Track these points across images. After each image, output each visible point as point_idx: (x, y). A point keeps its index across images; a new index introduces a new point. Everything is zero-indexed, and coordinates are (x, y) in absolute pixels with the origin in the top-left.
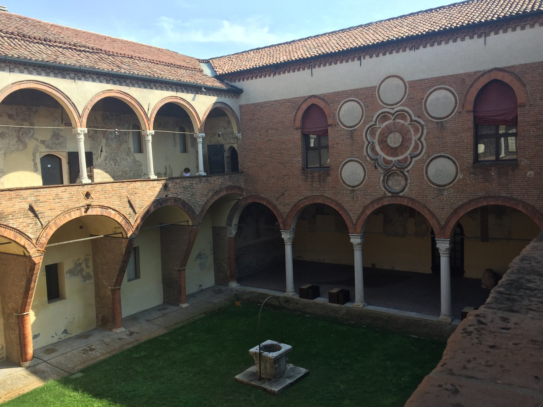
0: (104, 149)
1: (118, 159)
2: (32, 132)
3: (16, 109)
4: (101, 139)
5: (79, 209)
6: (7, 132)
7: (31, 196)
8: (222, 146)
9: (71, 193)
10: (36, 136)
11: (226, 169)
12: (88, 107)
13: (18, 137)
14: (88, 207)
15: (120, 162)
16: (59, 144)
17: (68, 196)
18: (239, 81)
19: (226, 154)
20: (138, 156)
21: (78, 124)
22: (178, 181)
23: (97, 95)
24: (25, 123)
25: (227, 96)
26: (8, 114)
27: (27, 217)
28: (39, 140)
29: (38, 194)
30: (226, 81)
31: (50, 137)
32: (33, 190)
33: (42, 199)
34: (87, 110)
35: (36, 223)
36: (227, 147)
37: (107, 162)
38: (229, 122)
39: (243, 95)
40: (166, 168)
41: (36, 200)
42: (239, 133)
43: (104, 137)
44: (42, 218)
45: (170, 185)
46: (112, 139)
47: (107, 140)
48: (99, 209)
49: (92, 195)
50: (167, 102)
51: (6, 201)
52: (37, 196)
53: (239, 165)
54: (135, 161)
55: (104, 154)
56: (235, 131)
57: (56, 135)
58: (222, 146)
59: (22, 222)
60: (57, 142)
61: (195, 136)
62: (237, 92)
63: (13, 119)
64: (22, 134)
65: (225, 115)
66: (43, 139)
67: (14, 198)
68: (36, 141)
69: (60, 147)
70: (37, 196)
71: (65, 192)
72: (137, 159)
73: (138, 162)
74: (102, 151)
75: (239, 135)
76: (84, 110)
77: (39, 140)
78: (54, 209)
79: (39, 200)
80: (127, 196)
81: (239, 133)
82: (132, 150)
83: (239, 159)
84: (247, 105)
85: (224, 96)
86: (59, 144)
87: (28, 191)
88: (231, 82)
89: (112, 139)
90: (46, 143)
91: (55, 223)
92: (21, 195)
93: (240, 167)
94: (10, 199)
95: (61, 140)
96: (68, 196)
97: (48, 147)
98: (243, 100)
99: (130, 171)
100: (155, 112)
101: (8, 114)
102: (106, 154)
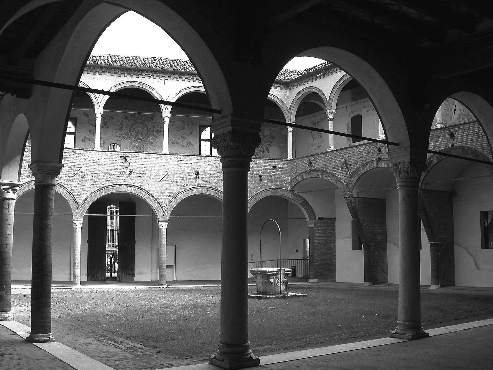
5: (372, 162)
14: (379, 160)
22: (468, 127)
27: (343, 169)
33: (351, 155)
35: (347, 173)
44: (350, 169)
48: (386, 162)
49: (382, 151)
59: (340, 172)
71: (365, 149)
74: (455, 110)
78: (358, 163)
79: (350, 156)
87: (345, 151)
91: (357, 173)
102: (460, 112)
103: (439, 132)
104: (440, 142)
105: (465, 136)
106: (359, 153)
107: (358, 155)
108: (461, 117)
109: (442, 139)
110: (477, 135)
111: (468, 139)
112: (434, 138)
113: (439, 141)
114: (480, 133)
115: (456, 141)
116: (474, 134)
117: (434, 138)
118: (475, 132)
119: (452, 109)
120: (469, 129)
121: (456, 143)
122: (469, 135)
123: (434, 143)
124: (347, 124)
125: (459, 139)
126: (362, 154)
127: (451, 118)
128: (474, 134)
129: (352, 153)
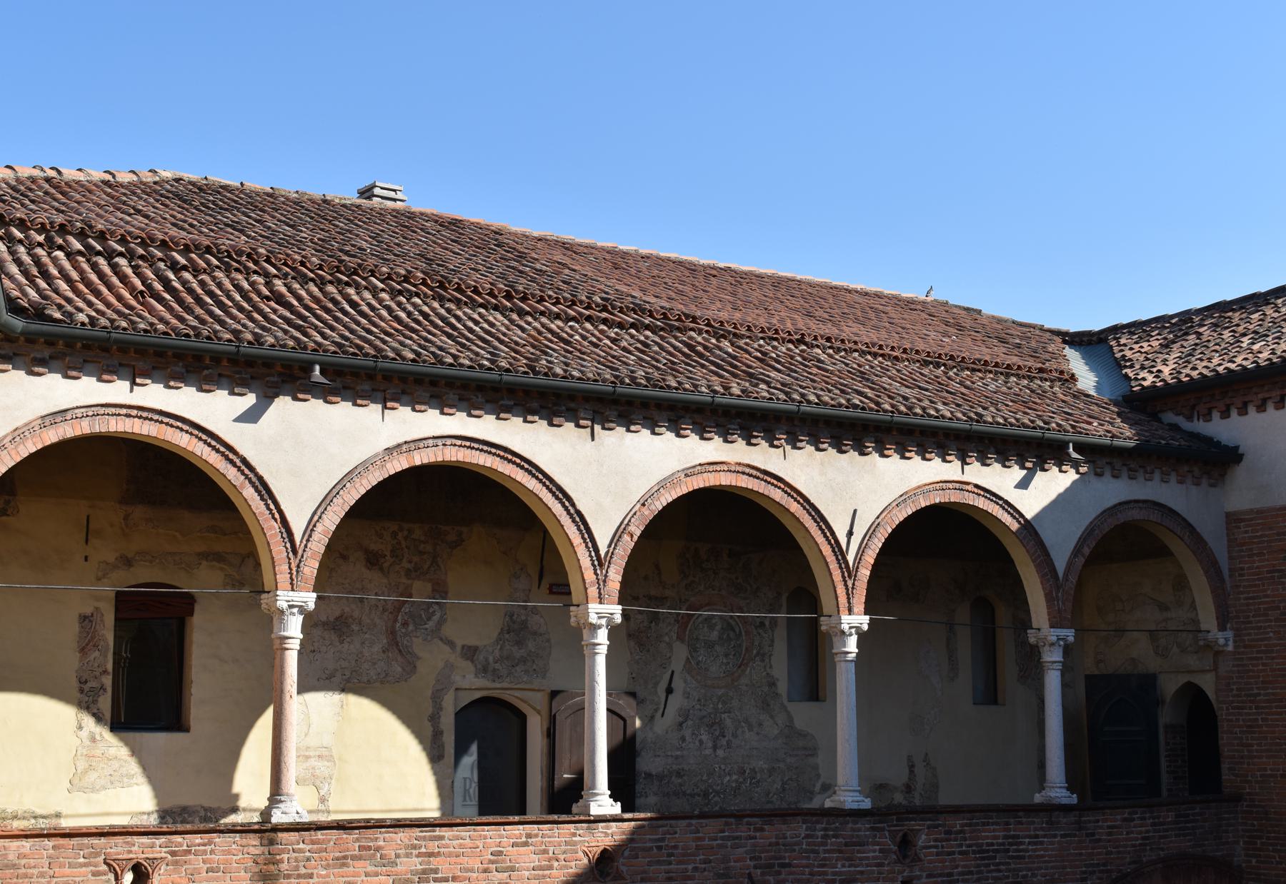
0: (678, 684)
1: (728, 722)
2: (436, 618)
3: (394, 535)
4: (670, 645)
6: (356, 614)
7: (407, 855)
8: (1149, 681)
9: (545, 852)
10: (448, 630)
11: (1165, 778)
12: (632, 528)
13: (392, 633)
15: (735, 736)
16: (523, 660)
17: (535, 860)
18: (1225, 414)
19: (1166, 717)
20: (803, 714)
21: (593, 591)
22: (957, 823)
23: (662, 485)
24: (417, 585)
25: (1173, 478)
26: (367, 552)
28: (459, 643)
29: (433, 846)
30: (1169, 417)
31: (495, 635)
32: (416, 832)
34: (626, 537)
36: (1170, 686)
37: (687, 733)
38: (1181, 583)
39: (1240, 473)
40: (911, 767)
41: (424, 872)
42: (1222, 628)
43: (680, 638)
45: (922, 840)
46: (710, 645)
47: (693, 649)
50: (923, 503)
51: (327, 867)
52: (431, 855)
53: (1225, 767)
54: (791, 732)
55: (676, 702)
56: (1208, 620)
57: (516, 629)
58: (1149, 681)
60: (518, 653)
61: (1032, 640)
62: (1219, 460)
63: (381, 569)
64: (405, 624)
65: (1163, 552)
66: (472, 641)
67: (354, 858)
68: (447, 648)
69: (526, 672)
70: (431, 855)
71: (526, 844)
72: (799, 724)
73: (802, 735)
74: (669, 691)
75: (1224, 639)
76: (615, 539)
77: (459, 643)
79: (436, 871)
80: (750, 875)
81: (1222, 628)
82: (782, 687)
83: (1224, 739)
84: (1260, 512)
85: (1157, 475)
86: (523, 660)
87: (403, 836)
88: (1190, 418)
89: (710, 645)
90: (481, 657)
92: (378, 849)
93: (1226, 776)
94: (342, 861)
95: (531, 645)
96: (535, 860)
97: (484, 670)
98: (1241, 494)
99: (772, 771)
100: (877, 543)
101: (367, 552)
103: (863, 826)
104: (867, 865)
105: (949, 854)
106: (492, 862)
107: (485, 871)
108: (690, 723)
109: (872, 852)
110: (983, 859)
111: (957, 867)
112: (846, 845)
113: (861, 859)
114: (993, 851)
115: (921, 870)
116: (974, 852)
117: (846, 845)
118: (977, 845)
119: (656, 684)
120: (961, 832)
121: (919, 878)
122: (961, 853)
123: (843, 866)
124: (84, 618)
125: (930, 862)
126: (512, 869)
127: (652, 717)
128: (974, 852)
129: (450, 855)
